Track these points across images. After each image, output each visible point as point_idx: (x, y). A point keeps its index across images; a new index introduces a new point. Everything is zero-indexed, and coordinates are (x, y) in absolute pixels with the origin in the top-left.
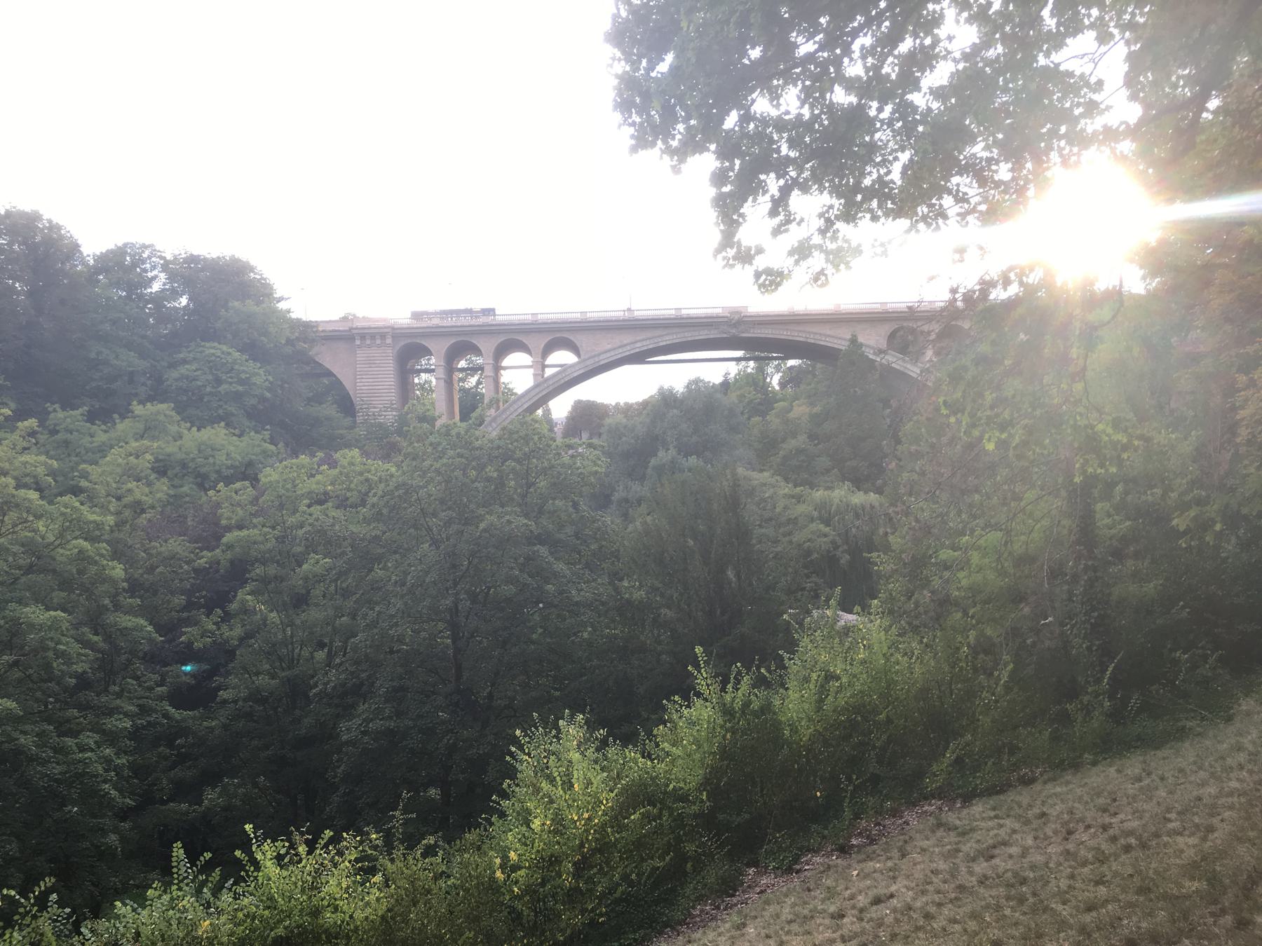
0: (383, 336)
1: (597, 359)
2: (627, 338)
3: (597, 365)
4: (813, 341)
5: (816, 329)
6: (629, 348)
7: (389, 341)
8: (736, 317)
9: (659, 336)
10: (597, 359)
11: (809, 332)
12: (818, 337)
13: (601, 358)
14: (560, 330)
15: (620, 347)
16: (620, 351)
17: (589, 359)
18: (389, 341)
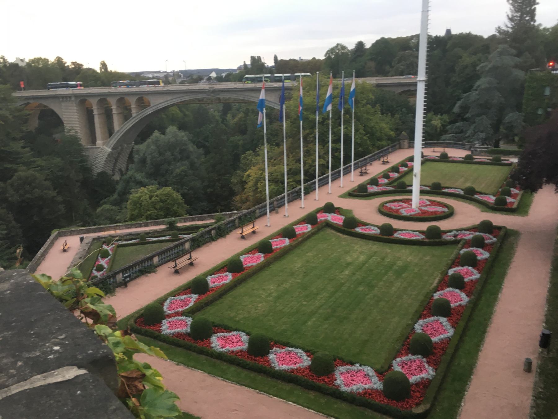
0: (70, 97)
1: (157, 106)
2: (169, 98)
3: (157, 109)
4: (247, 99)
5: (247, 94)
6: (169, 102)
7: (73, 99)
8: (212, 89)
9: (182, 97)
10: (157, 106)
11: (246, 95)
12: (249, 97)
13: (160, 105)
14: (142, 94)
15: (166, 101)
16: (166, 103)
17: (154, 106)
18: (73, 99)
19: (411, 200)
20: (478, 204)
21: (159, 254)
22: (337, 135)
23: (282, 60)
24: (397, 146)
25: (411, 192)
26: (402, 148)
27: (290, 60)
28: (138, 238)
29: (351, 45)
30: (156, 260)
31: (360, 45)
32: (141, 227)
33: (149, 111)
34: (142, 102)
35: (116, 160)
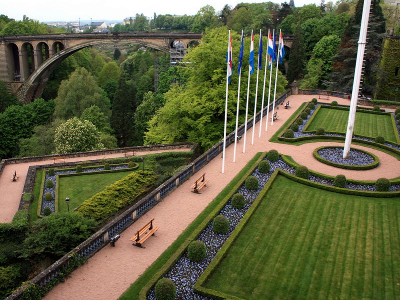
19: (343, 148)
20: (369, 146)
21: (137, 209)
22: (261, 83)
23: (160, 16)
24: (290, 93)
25: (344, 140)
26: (294, 94)
27: (167, 15)
28: (75, 170)
29: (218, 9)
30: (135, 214)
31: (226, 9)
32: (74, 157)
33: (63, 53)
34: (59, 45)
35: (35, 92)
